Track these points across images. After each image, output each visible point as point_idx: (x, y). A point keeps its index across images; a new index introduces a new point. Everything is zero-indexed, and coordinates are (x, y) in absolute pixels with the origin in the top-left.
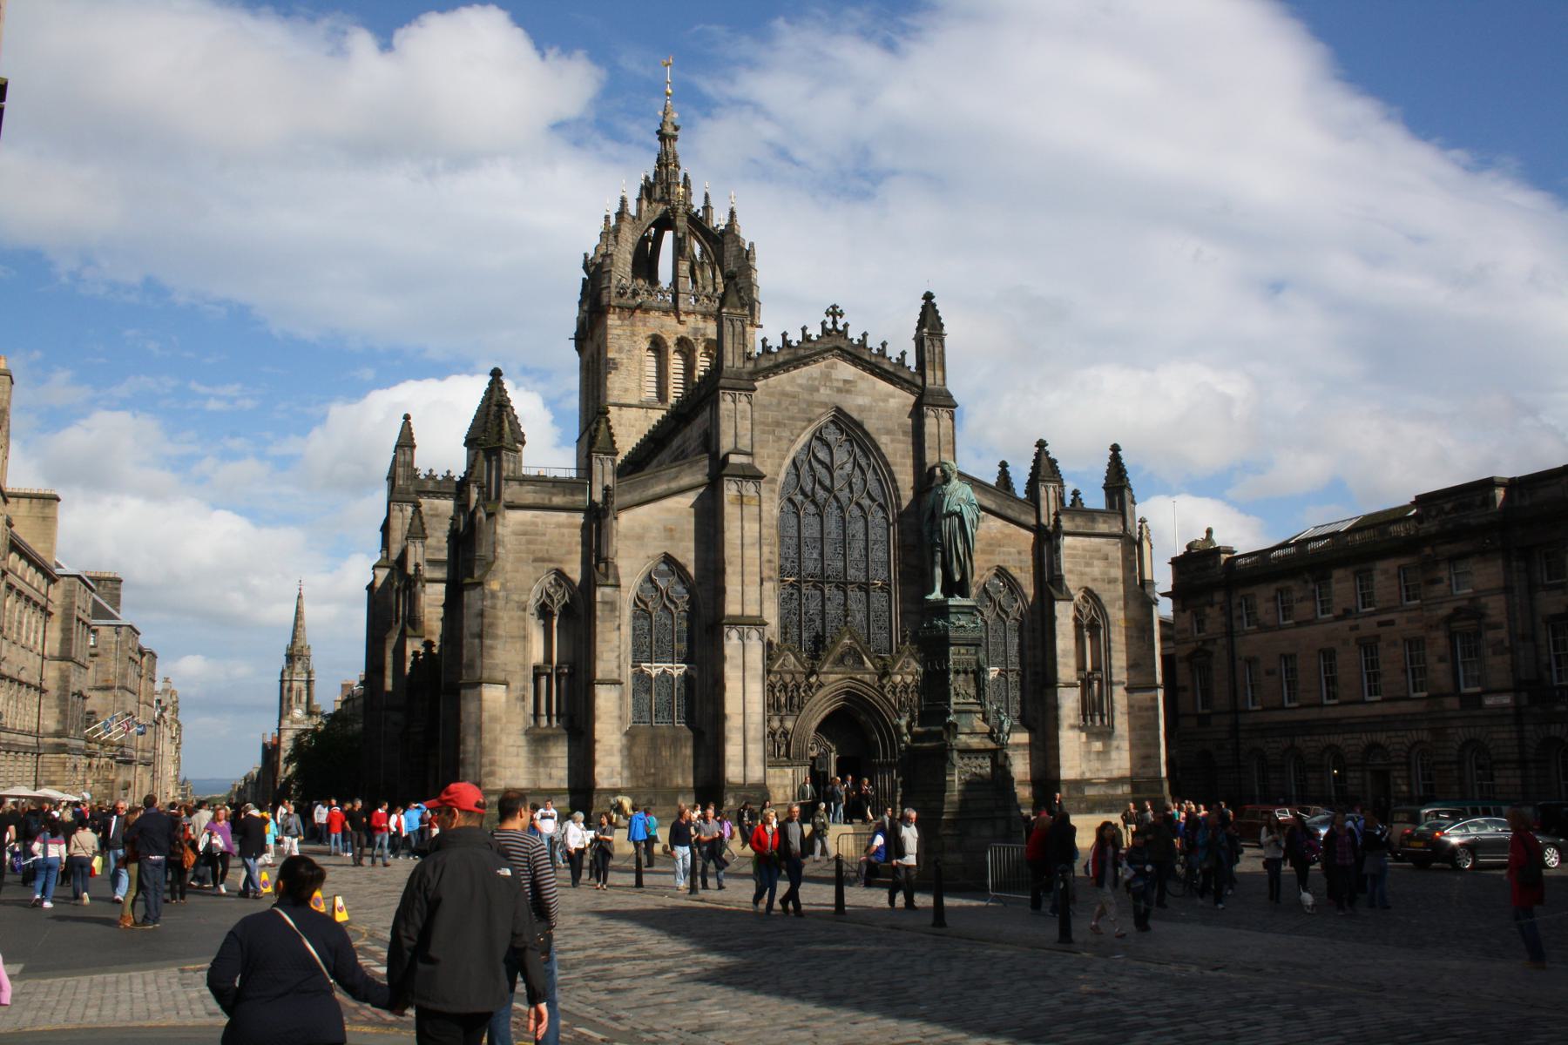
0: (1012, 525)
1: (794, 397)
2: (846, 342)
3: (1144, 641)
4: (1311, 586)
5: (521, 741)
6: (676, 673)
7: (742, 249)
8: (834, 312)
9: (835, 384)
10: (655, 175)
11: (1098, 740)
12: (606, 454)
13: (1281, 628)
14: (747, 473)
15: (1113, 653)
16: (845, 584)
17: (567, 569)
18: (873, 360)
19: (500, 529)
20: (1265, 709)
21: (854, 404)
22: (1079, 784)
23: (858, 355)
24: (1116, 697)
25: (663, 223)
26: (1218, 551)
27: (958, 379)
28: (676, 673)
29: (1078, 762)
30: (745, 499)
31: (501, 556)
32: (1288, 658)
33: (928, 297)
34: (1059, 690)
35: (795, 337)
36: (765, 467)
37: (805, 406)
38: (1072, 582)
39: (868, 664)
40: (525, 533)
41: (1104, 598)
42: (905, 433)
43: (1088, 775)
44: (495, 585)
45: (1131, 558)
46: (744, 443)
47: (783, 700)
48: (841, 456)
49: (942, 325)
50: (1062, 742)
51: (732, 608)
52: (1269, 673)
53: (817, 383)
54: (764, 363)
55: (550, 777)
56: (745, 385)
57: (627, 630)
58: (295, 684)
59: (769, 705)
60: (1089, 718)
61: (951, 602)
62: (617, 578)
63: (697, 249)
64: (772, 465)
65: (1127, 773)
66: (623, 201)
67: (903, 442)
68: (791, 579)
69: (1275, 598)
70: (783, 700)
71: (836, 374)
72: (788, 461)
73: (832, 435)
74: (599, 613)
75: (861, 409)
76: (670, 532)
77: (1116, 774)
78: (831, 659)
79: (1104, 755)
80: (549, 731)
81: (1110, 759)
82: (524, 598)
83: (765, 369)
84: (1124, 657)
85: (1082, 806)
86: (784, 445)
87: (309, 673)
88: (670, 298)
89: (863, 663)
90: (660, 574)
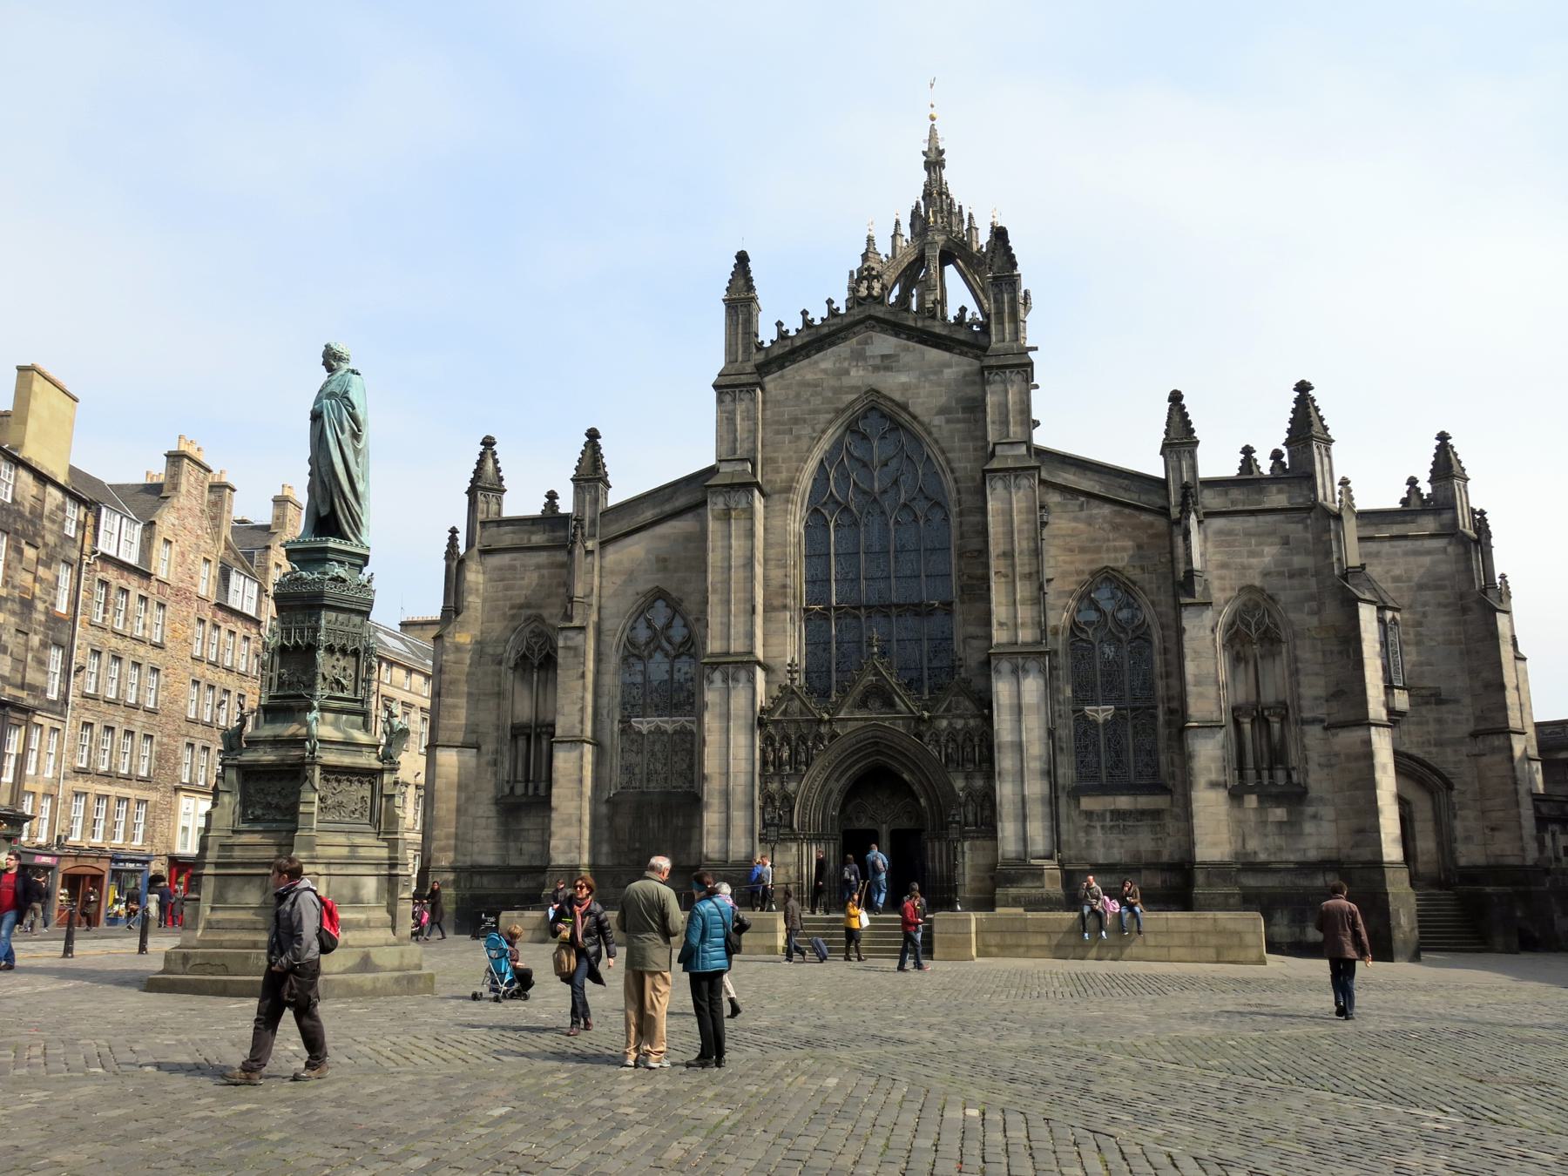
0: (1127, 511)
1: (816, 386)
2: (883, 309)
3: (1348, 657)
6: (669, 728)
9: (871, 362)
11: (1278, 806)
12: (587, 480)
14: (736, 481)
15: (1303, 679)
16: (889, 606)
17: (545, 613)
18: (920, 324)
21: (893, 383)
24: (1307, 741)
28: (669, 728)
29: (1224, 835)
30: (733, 513)
31: (472, 605)
34: (1190, 733)
37: (830, 395)
39: (902, 707)
41: (1283, 597)
42: (965, 410)
43: (1262, 857)
45: (1325, 538)
49: (1014, 265)
50: (1195, 806)
51: (714, 645)
53: (846, 364)
54: (777, 351)
55: (521, 852)
59: (764, 763)
60: (1265, 774)
64: (788, 470)
65: (1334, 855)
66: (870, 240)
67: (964, 421)
68: (817, 607)
70: (785, 755)
73: (871, 426)
74: (560, 660)
75: (905, 388)
76: (662, 563)
77: (1313, 855)
78: (850, 701)
79: (1291, 827)
80: (524, 800)
81: (1301, 834)
82: (500, 650)
83: (778, 358)
84: (1321, 682)
85: (1232, 901)
86: (804, 444)
89: (892, 705)
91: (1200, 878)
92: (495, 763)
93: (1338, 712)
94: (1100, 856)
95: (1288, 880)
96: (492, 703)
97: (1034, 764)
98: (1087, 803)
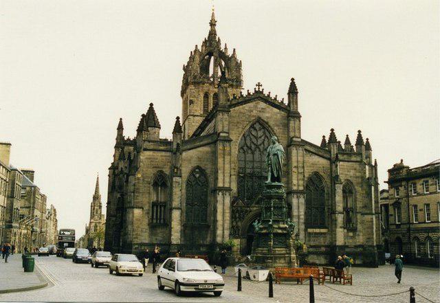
4: (435, 180)
5: (147, 227)
7: (237, 63)
8: (259, 85)
10: (209, 37)
13: (425, 195)
17: (164, 170)
19: (141, 157)
20: (419, 223)
21: (265, 116)
22: (343, 247)
23: (267, 100)
25: (210, 54)
26: (404, 167)
27: (302, 109)
32: (428, 205)
33: (293, 79)
35: (245, 93)
36: (233, 137)
38: (342, 178)
40: (150, 159)
43: (347, 244)
44: (139, 176)
46: (226, 129)
47: (237, 215)
48: (260, 133)
51: (220, 184)
52: (421, 210)
54: (234, 102)
56: (226, 110)
57: (184, 191)
58: (96, 207)
61: (273, 184)
62: (181, 173)
63: (223, 63)
65: (361, 244)
69: (423, 184)
70: (237, 215)
71: (259, 106)
72: (242, 135)
73: (257, 126)
75: (268, 118)
86: (240, 129)
87: (100, 204)
88: (212, 79)
90: (197, 173)
91: (337, 250)
92: (148, 213)
93: (365, 211)
94: (312, 244)
95: (353, 249)
96: (147, 196)
97: (302, 221)
98: (310, 230)
